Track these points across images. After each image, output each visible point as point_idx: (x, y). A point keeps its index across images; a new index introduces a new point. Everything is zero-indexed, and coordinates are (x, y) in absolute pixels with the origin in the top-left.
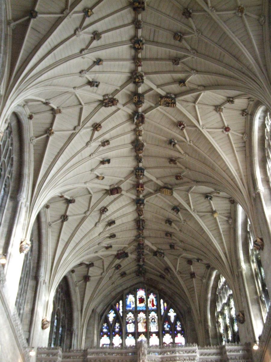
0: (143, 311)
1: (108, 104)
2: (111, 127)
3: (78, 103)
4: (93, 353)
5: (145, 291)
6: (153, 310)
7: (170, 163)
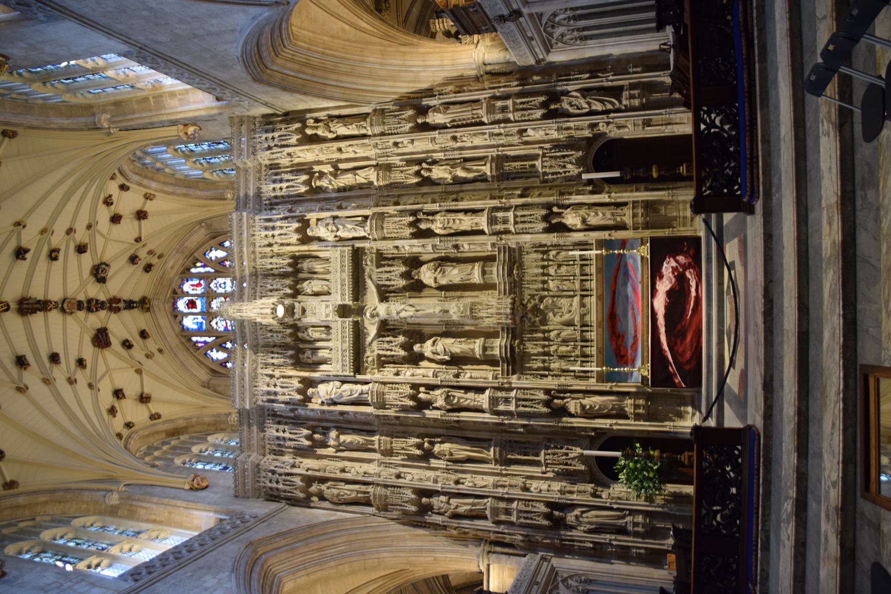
4: (243, 400)
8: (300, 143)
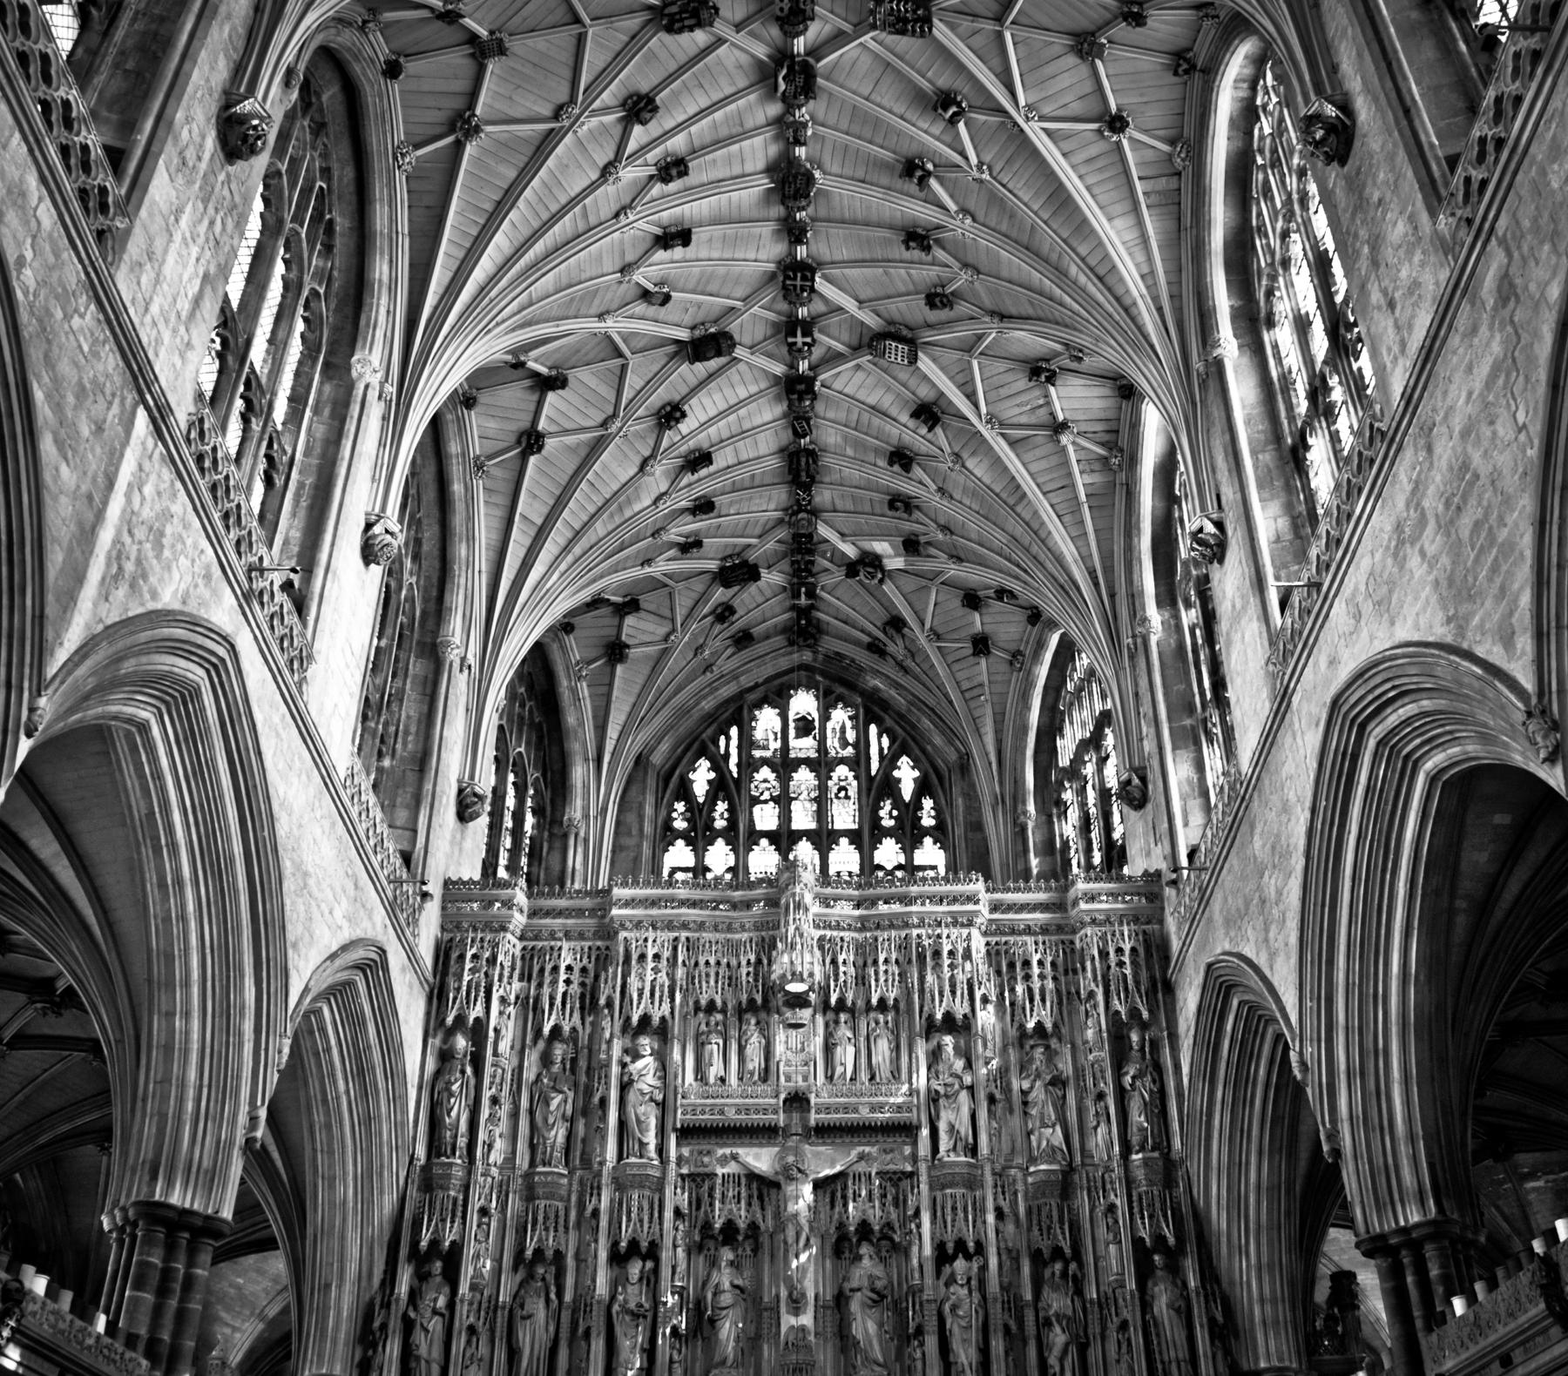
0: (807, 762)
1: (682, 20)
2: (692, 110)
3: (568, 18)
4: (629, 903)
5: (817, 697)
6: (842, 761)
7: (908, 248)
8: (1113, 1016)
